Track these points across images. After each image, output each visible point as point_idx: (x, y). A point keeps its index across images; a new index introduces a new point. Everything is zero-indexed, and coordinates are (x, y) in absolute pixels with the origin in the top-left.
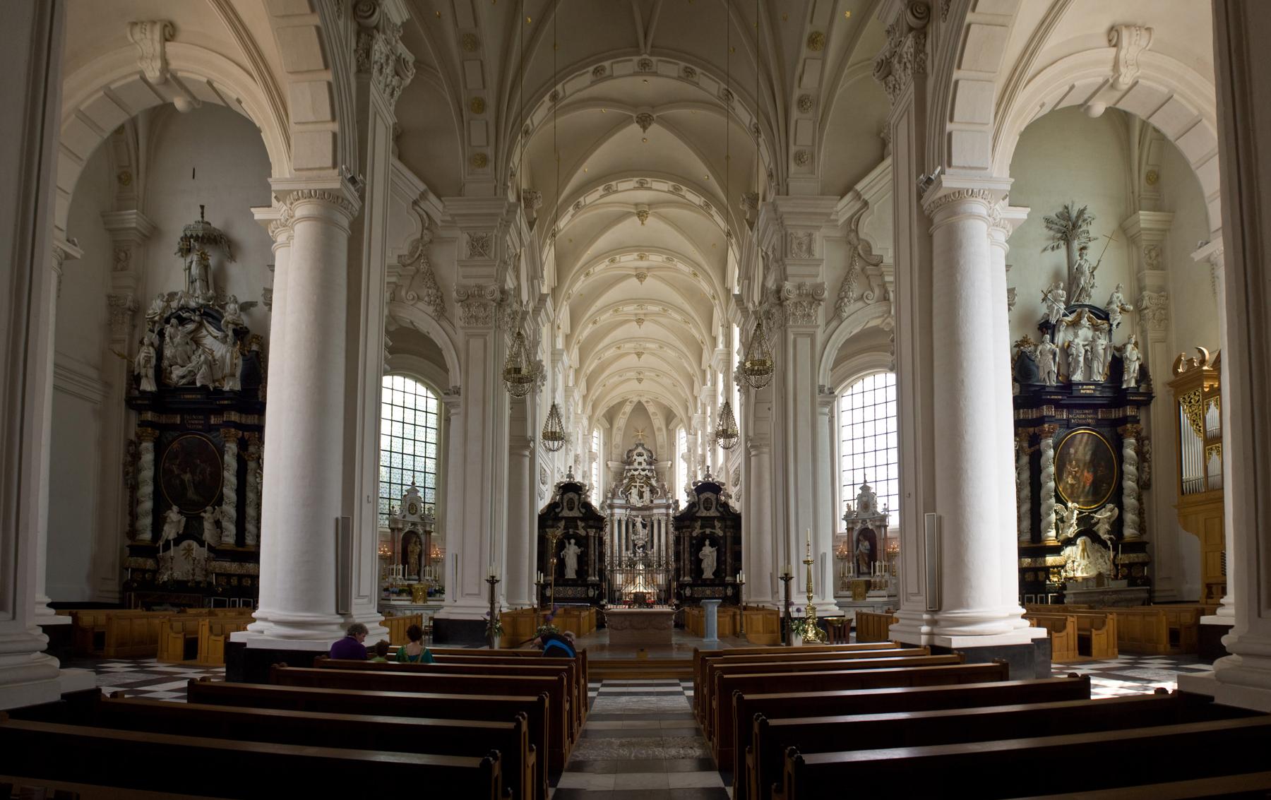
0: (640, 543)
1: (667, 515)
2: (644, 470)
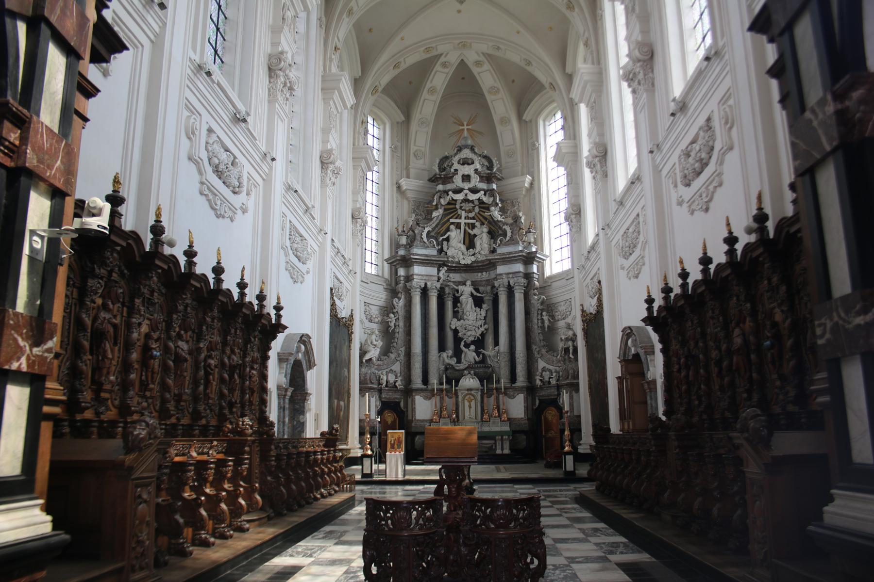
0: (470, 335)
1: (528, 276)
2: (474, 191)
